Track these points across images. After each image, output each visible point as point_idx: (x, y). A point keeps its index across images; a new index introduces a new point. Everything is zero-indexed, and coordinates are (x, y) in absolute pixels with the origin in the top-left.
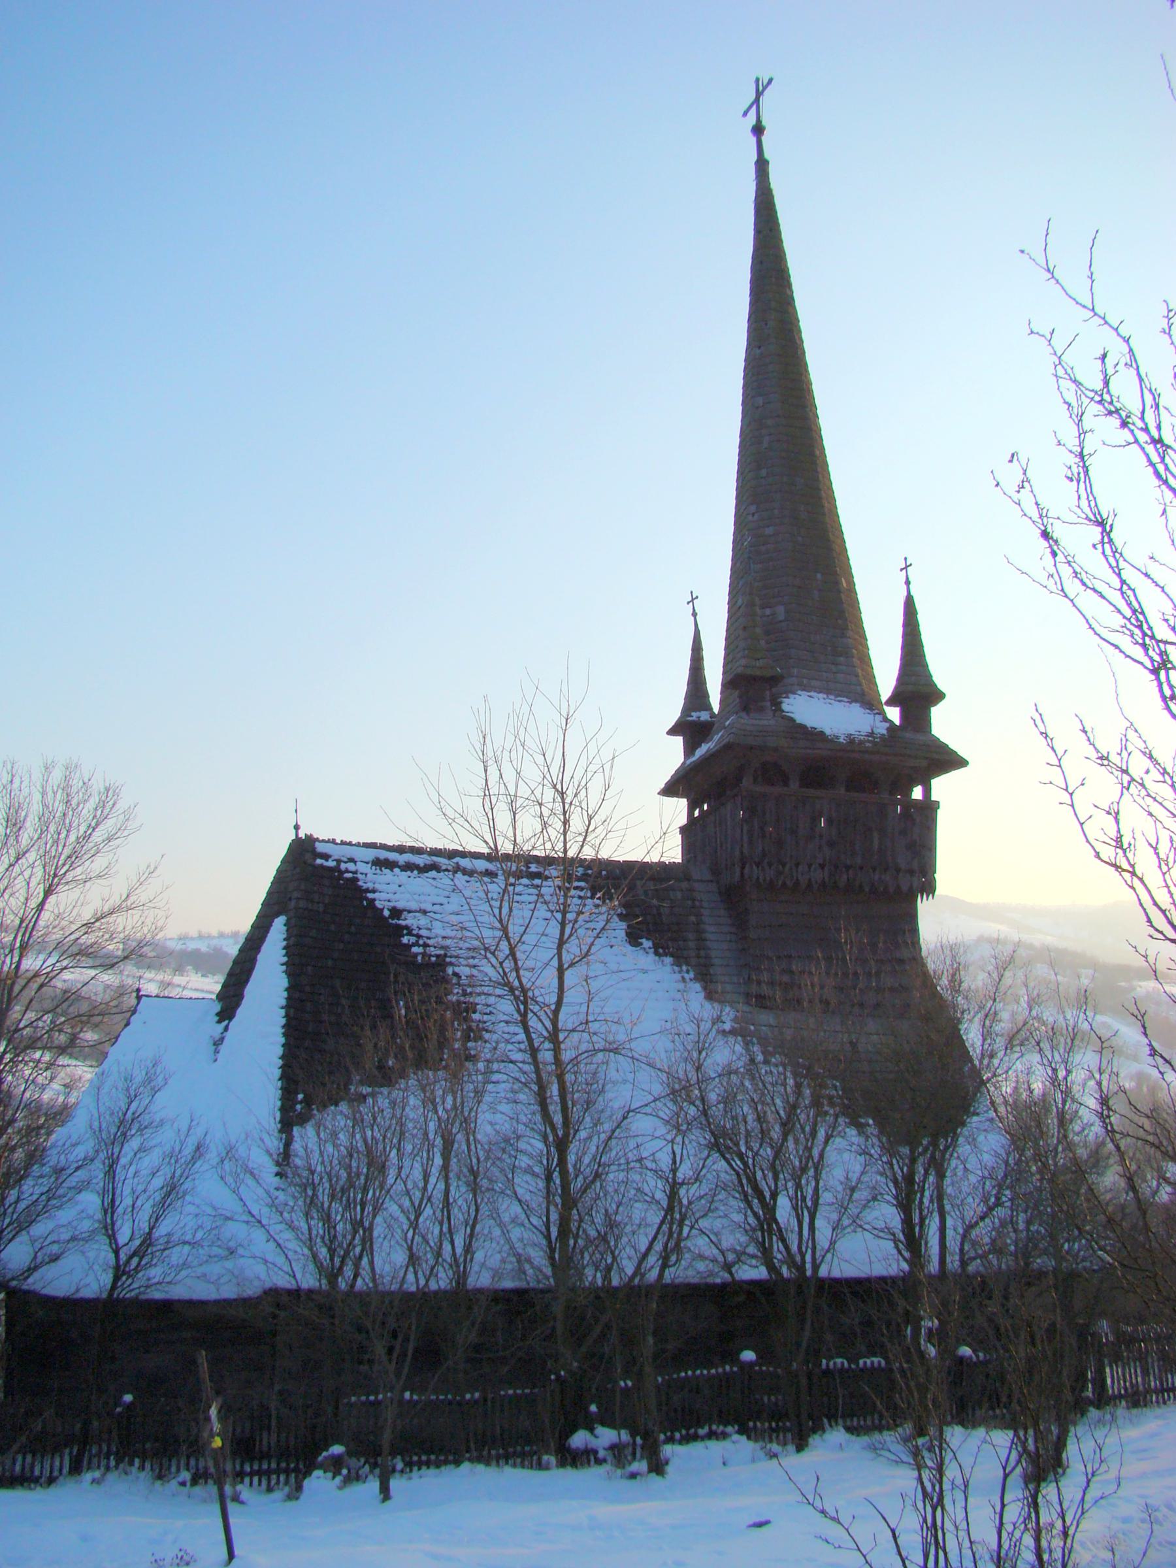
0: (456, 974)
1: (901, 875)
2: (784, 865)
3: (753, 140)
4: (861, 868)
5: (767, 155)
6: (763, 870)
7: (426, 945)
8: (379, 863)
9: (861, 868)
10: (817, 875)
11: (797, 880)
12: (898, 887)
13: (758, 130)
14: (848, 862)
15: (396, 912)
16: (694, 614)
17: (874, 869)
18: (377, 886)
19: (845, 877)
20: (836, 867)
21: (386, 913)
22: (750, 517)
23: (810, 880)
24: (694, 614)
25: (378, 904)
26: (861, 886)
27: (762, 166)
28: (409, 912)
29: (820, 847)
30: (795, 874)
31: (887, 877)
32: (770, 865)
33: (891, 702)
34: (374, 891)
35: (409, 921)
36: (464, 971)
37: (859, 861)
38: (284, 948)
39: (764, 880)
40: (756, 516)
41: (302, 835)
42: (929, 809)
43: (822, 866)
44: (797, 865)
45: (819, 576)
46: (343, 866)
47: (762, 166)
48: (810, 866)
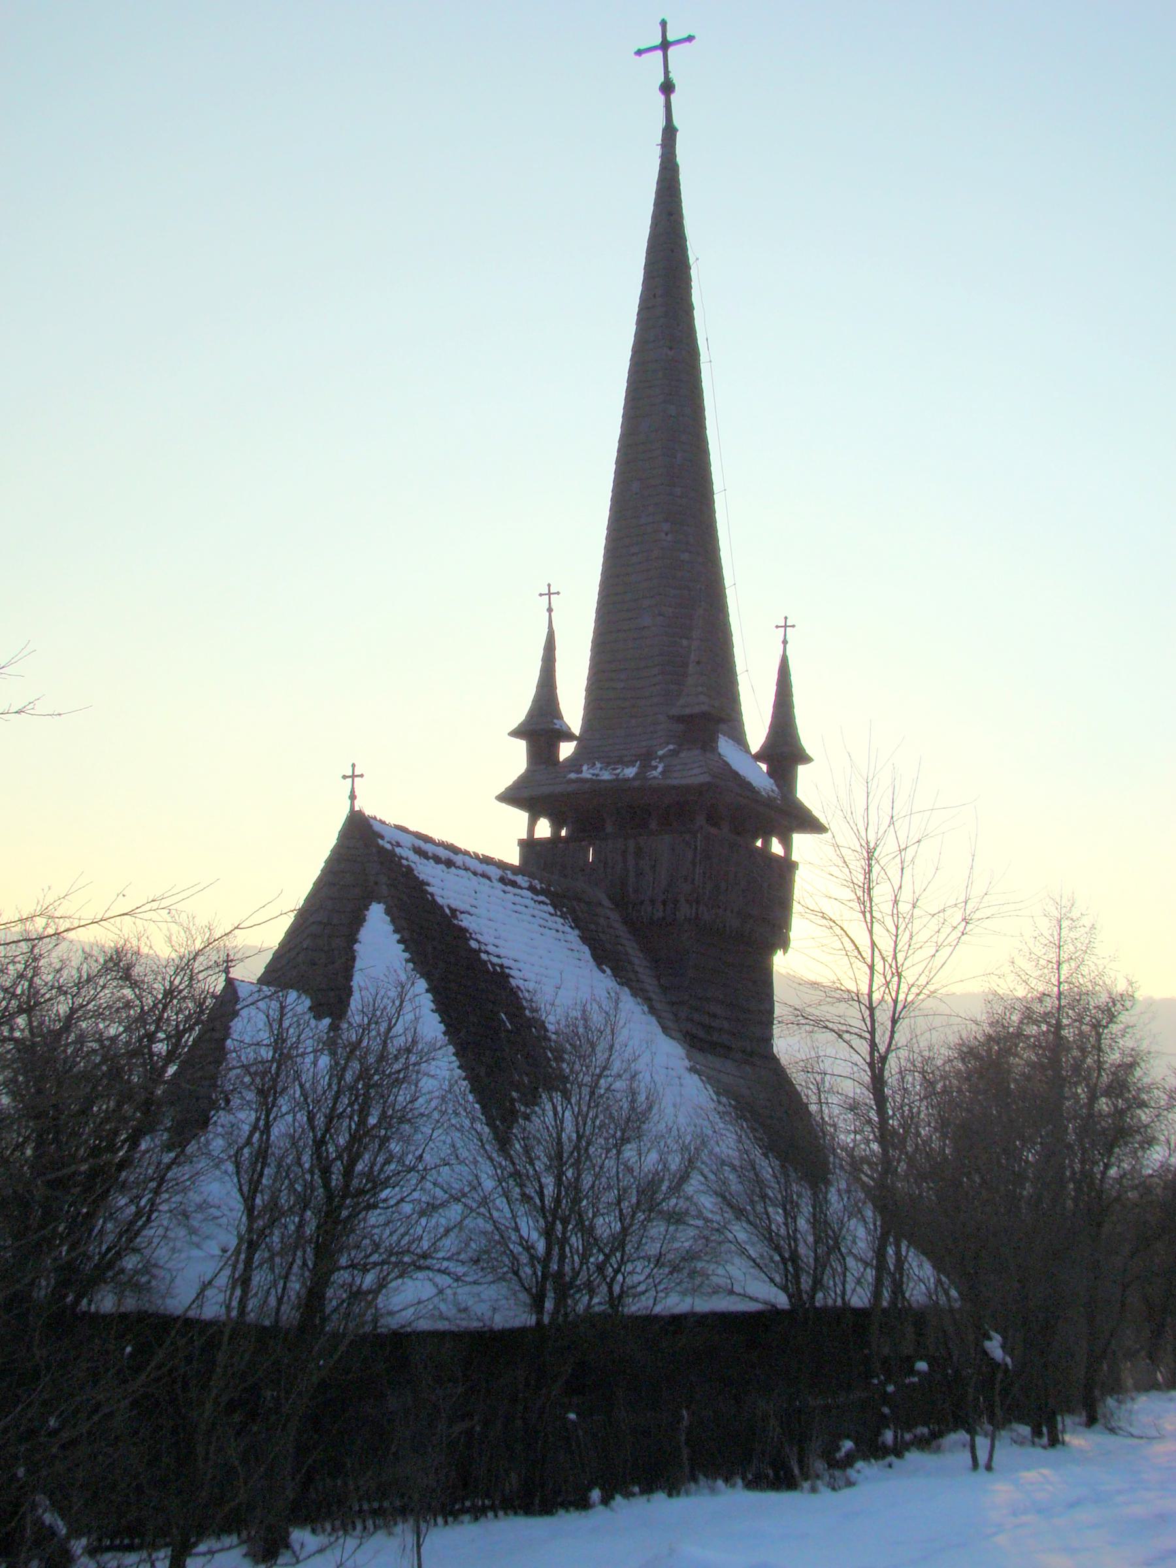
0: (518, 987)
3: (661, 99)
5: (676, 122)
7: (487, 953)
8: (419, 851)
13: (667, 88)
15: (454, 911)
16: (550, 610)
18: (431, 880)
21: (447, 911)
22: (663, 535)
24: (550, 610)
25: (440, 900)
27: (669, 134)
28: (462, 913)
33: (758, 757)
34: (428, 885)
35: (465, 922)
36: (521, 983)
38: (399, 942)
40: (669, 537)
41: (357, 808)
42: (785, 869)
46: (398, 850)
47: (669, 134)
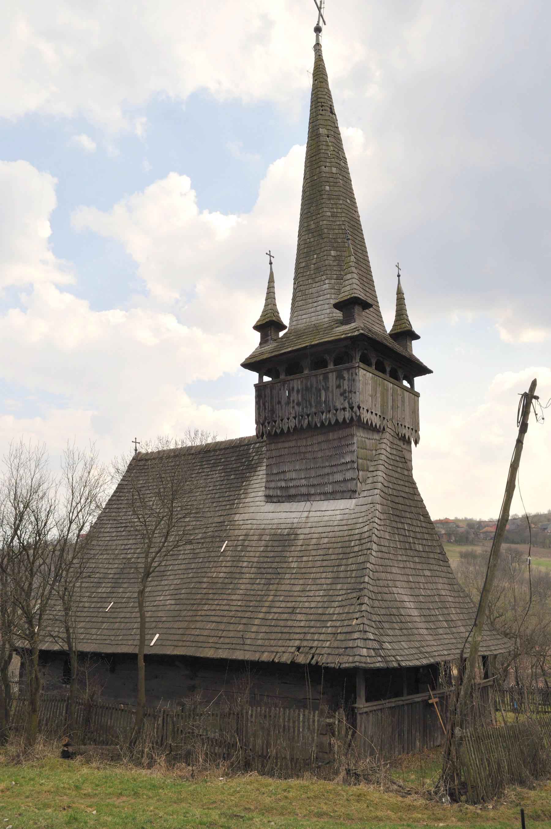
1: (338, 412)
2: (275, 422)
4: (315, 414)
6: (265, 427)
9: (315, 414)
10: (292, 423)
11: (282, 429)
12: (337, 420)
14: (308, 413)
17: (322, 413)
19: (306, 421)
20: (302, 417)
23: (289, 428)
26: (316, 425)
27: (317, 47)
29: (293, 407)
30: (281, 426)
31: (330, 416)
32: (269, 423)
37: (314, 410)
39: (266, 432)
43: (295, 418)
44: (282, 420)
45: (315, 256)
47: (317, 47)
48: (288, 419)
